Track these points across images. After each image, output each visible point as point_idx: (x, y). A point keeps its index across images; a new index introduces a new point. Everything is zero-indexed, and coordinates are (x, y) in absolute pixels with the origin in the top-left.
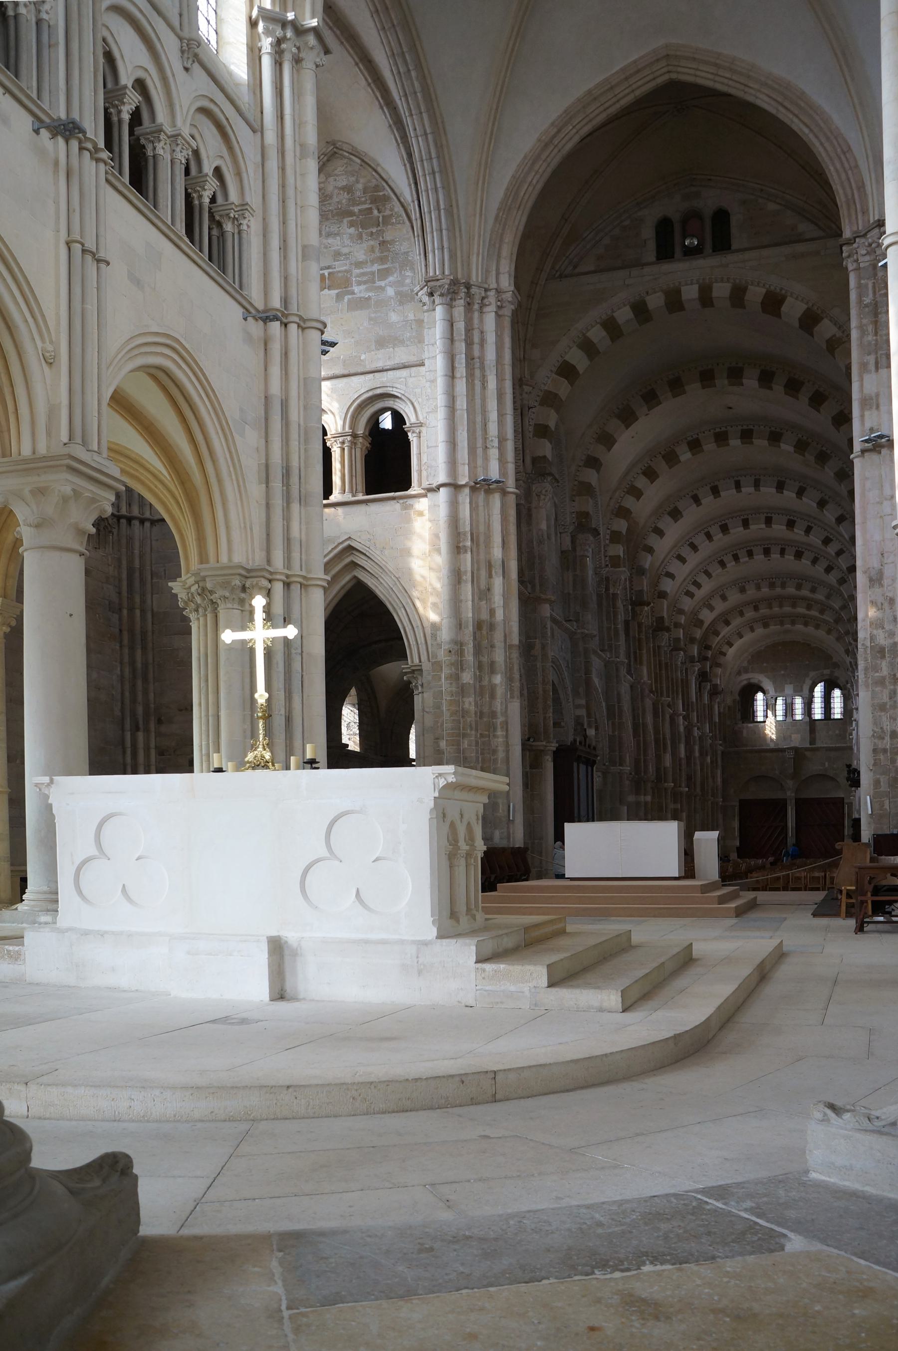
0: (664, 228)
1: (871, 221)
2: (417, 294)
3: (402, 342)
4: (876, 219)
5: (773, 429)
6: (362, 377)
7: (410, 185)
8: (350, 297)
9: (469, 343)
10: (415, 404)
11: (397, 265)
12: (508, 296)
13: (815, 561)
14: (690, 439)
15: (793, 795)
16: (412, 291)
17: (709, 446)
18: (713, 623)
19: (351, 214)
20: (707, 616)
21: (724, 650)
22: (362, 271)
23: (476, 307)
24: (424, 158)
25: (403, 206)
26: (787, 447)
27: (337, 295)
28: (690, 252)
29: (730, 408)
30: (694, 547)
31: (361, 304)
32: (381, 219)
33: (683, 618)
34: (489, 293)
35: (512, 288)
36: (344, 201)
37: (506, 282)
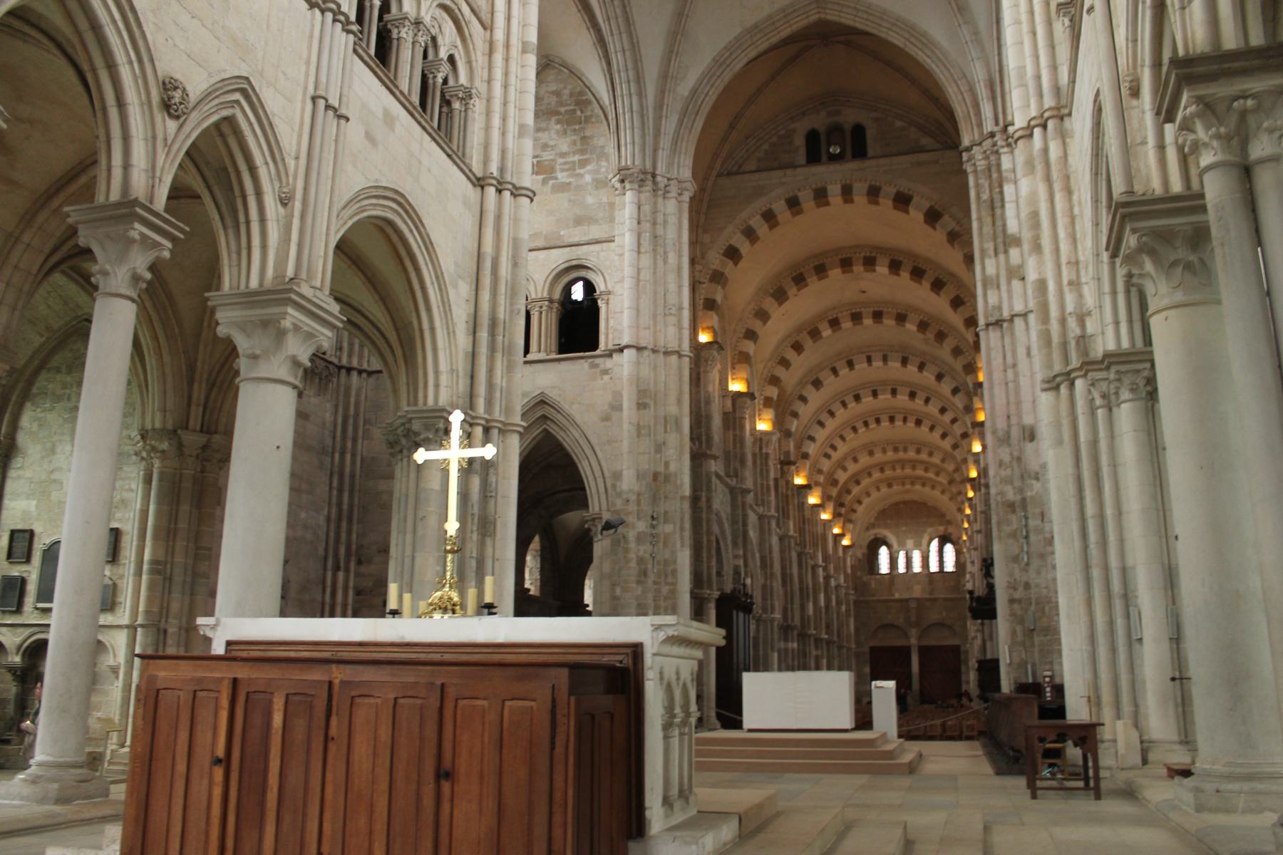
0: (813, 139)
2: (610, 181)
3: (596, 221)
4: (989, 130)
6: (561, 249)
7: (608, 91)
8: (554, 181)
11: (594, 156)
14: (830, 318)
16: (606, 178)
17: (847, 325)
18: (846, 483)
19: (558, 113)
20: (842, 477)
22: (564, 160)
24: (621, 69)
25: (601, 108)
26: (911, 327)
27: (543, 180)
28: (833, 158)
31: (564, 187)
32: (583, 119)
34: (670, 182)
36: (553, 103)
37: (687, 173)
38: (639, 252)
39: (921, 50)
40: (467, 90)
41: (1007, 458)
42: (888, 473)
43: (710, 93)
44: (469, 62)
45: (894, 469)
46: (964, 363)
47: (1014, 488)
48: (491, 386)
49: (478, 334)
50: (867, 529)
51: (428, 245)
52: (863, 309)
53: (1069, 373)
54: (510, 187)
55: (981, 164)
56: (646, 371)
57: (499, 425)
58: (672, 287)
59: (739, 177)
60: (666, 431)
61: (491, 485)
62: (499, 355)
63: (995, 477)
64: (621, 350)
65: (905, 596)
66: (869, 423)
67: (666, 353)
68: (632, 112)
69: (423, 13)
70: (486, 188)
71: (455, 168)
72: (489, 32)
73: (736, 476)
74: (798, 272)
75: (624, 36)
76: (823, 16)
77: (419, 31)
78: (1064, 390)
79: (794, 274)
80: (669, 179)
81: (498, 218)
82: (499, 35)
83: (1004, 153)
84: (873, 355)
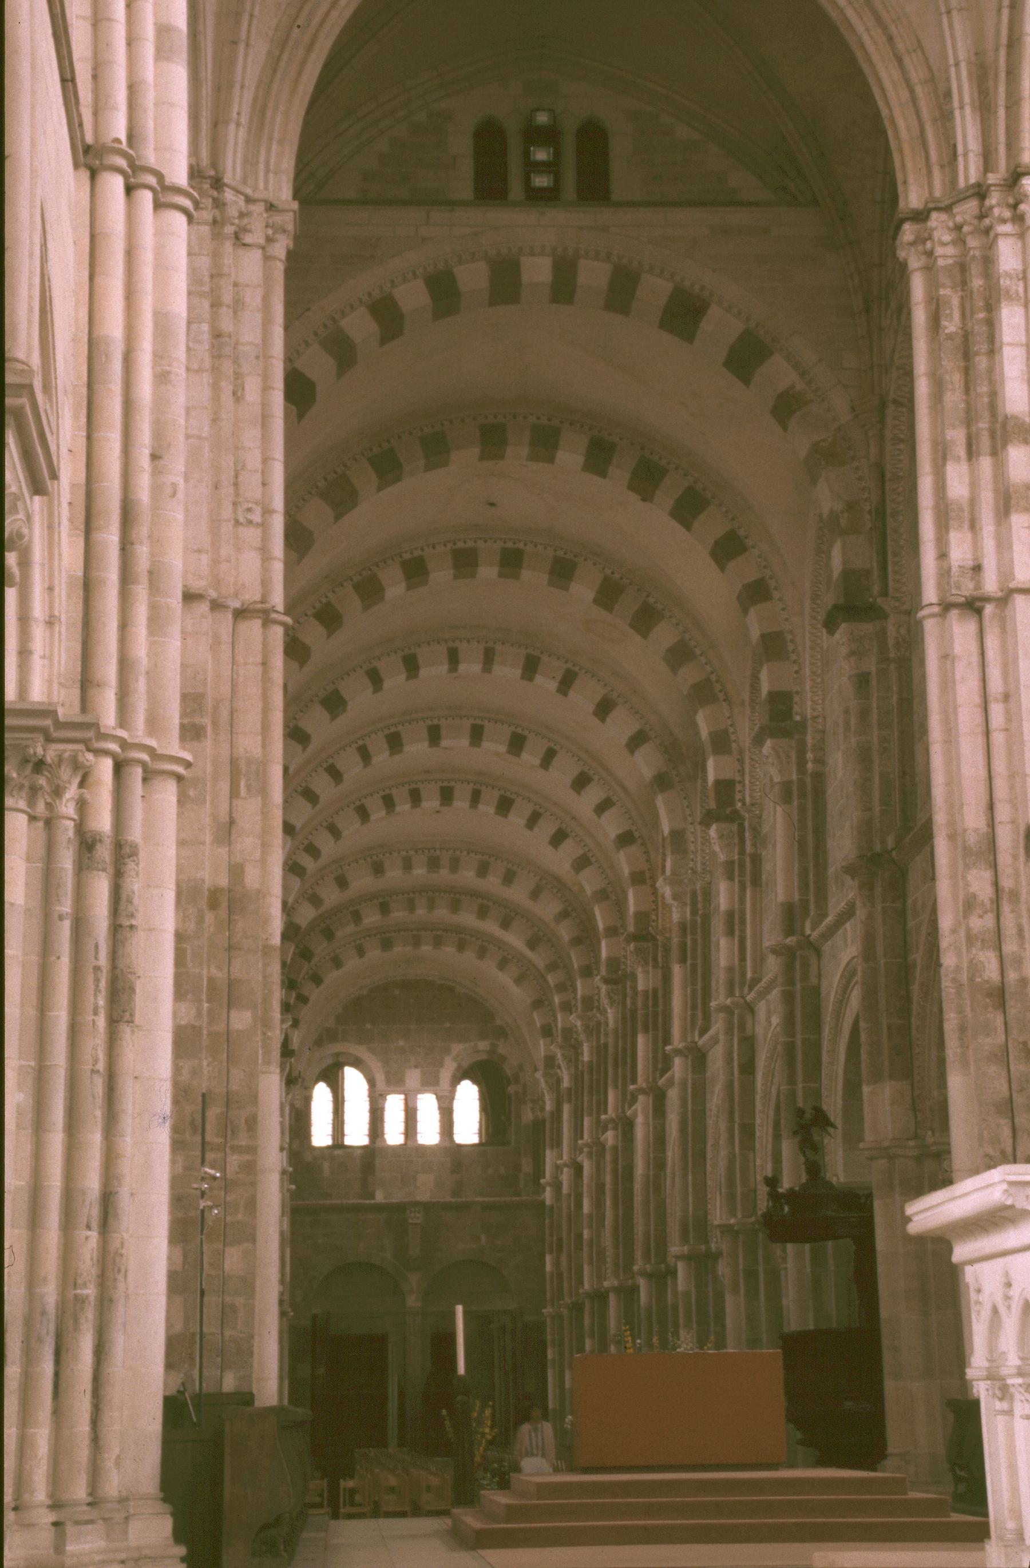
5: (560, 553)
12: (288, 221)
14: (407, 556)
15: (419, 1304)
17: (441, 575)
28: (536, 197)
29: (492, 505)
34: (253, 208)
35: (295, 206)
37: (283, 192)
42: (398, 915)
45: (411, 907)
48: (125, 664)
49: (98, 536)
50: (319, 1043)
52: (480, 544)
55: (946, 254)
57: (145, 757)
58: (253, 459)
60: (234, 793)
63: (954, 931)
65: (398, 1197)
66: (396, 800)
67: (241, 614)
80: (248, 200)
83: (1006, 235)
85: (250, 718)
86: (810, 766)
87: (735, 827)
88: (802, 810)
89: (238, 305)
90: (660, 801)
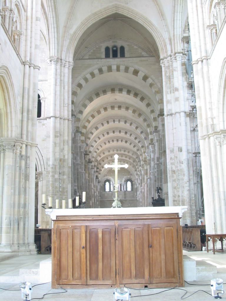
0: (107, 49)
1: (168, 55)
2: (46, 60)
4: (169, 54)
7: (46, 30)
9: (61, 76)
10: (44, 92)
12: (72, 64)
13: (130, 144)
14: (104, 107)
16: (45, 59)
21: (101, 169)
23: (63, 66)
26: (130, 111)
30: (99, 138)
33: (94, 159)
34: (66, 62)
35: (73, 62)
37: (71, 59)
38: (56, 85)
39: (149, 26)
40: (20, 32)
41: (173, 157)
43: (80, 34)
44: (21, 23)
46: (147, 124)
47: (175, 166)
48: (27, 131)
50: (104, 176)
51: (12, 85)
53: (208, 135)
54: (33, 65)
55: (167, 64)
56: (58, 125)
57: (30, 144)
58: (66, 97)
59: (83, 61)
60: (64, 145)
61: (28, 164)
62: (30, 121)
63: (169, 163)
64: (50, 118)
68: (55, 38)
69: (12, 8)
70: (26, 65)
71: (18, 58)
72: (26, 13)
73: (75, 159)
74: (97, 92)
75: (54, 12)
76: (117, 12)
77: (11, 13)
78: (207, 139)
79: (96, 93)
80: (66, 61)
81: (29, 75)
82: (29, 14)
83: (174, 62)
84: (115, 119)
85: (66, 134)
86: (160, 137)
87: (153, 145)
88: (159, 143)
89: (64, 76)
90: (145, 141)
